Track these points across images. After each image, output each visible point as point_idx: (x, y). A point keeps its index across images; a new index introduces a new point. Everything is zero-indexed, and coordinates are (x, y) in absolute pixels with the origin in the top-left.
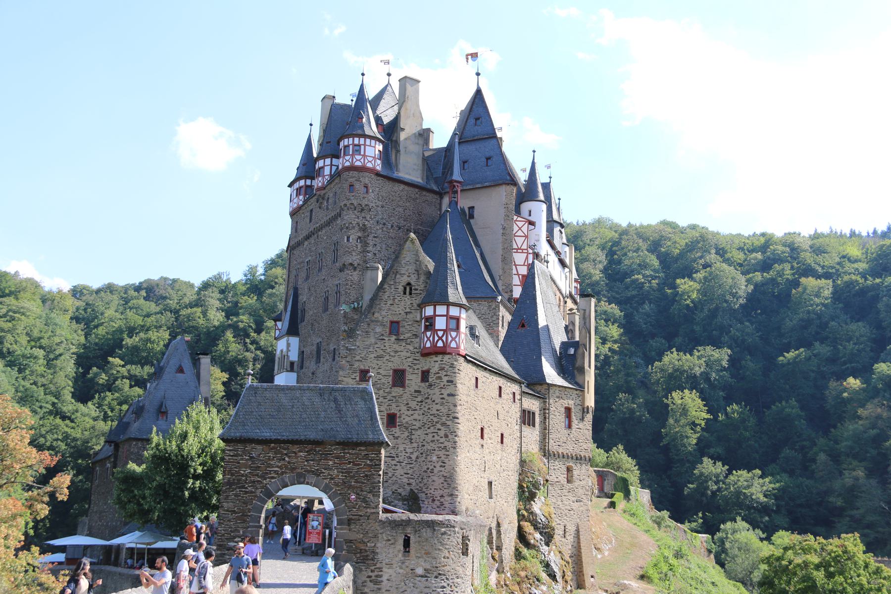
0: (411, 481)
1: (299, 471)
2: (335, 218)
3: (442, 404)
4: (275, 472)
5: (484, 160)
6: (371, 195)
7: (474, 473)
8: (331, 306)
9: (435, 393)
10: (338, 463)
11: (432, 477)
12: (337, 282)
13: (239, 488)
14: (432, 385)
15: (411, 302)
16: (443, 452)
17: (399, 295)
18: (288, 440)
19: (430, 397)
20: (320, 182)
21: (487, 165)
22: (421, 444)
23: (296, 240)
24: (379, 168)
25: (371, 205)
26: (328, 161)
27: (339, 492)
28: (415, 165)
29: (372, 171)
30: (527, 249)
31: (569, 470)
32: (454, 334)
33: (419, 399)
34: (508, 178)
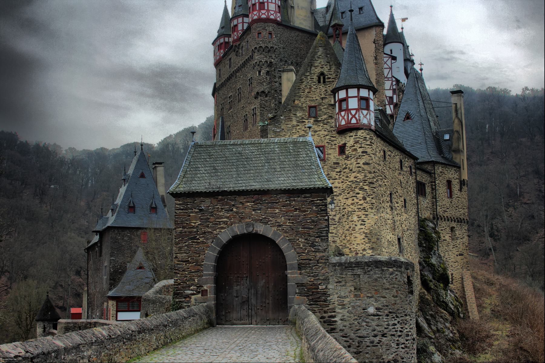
0: (336, 238)
1: (248, 220)
2: (248, 61)
3: (359, 172)
4: (224, 223)
5: (358, 10)
6: (275, 40)
7: (387, 231)
8: (250, 126)
9: (352, 163)
10: (284, 211)
11: (354, 234)
12: (252, 108)
13: (191, 239)
14: (349, 157)
15: (326, 89)
16: (363, 212)
17: (315, 84)
18: (235, 191)
19: (347, 167)
20: (235, 35)
21: (360, 13)
22: (342, 208)
23: (220, 83)
24: (278, 19)
25: (275, 47)
26: (240, 20)
27: (287, 238)
28: (305, 16)
29: (275, 21)
30: (391, 78)
31: (452, 229)
32: (365, 112)
33: (338, 170)
34: (377, 21)
